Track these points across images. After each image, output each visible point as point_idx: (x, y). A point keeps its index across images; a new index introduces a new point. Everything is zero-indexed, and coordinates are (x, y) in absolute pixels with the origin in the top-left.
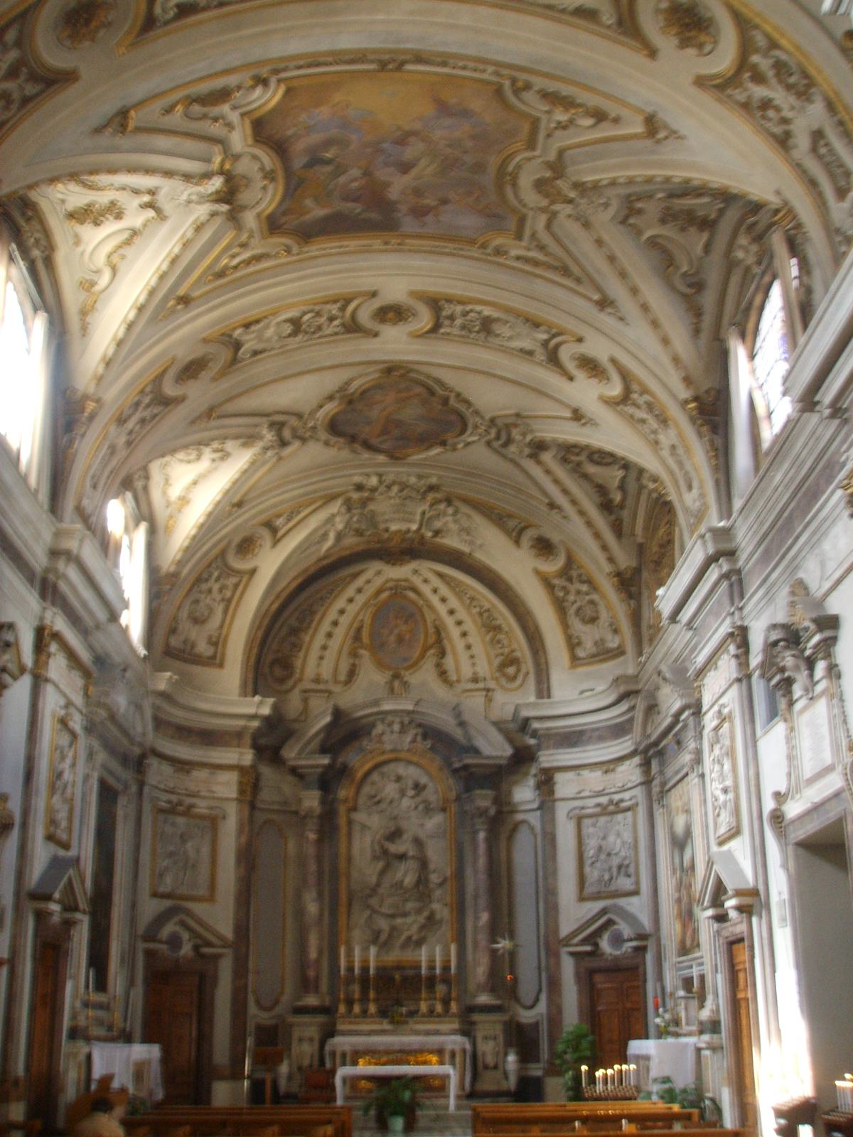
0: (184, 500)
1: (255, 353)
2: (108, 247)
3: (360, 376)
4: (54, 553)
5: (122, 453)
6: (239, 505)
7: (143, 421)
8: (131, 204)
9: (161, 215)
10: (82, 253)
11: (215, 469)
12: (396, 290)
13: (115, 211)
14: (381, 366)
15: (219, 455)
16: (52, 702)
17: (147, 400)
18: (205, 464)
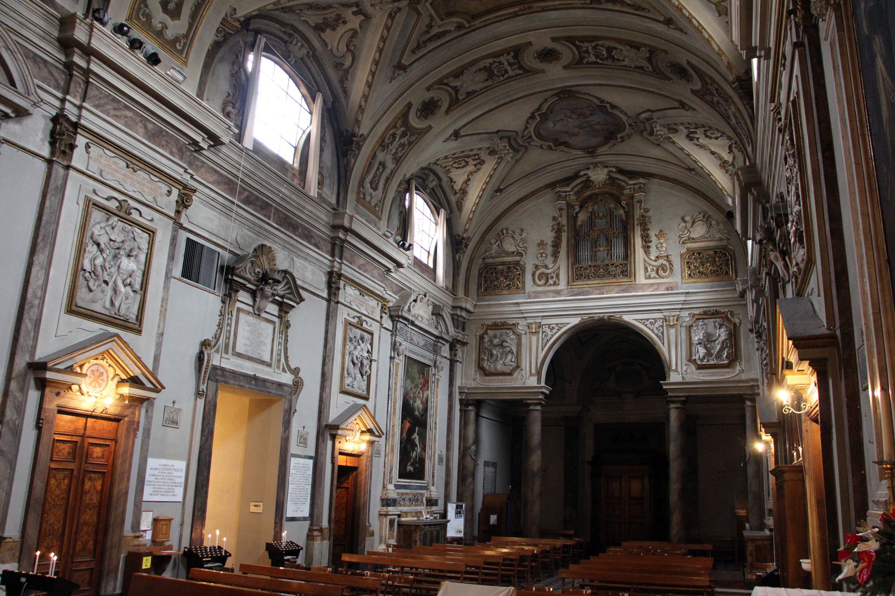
0: (464, 192)
1: (469, 94)
2: (345, 40)
3: (546, 100)
4: (335, 228)
5: (390, 165)
6: (499, 190)
7: (402, 145)
8: (348, 14)
9: (368, 17)
10: (331, 50)
11: (479, 169)
12: (542, 40)
13: (339, 20)
14: (554, 92)
15: (478, 161)
16: (343, 314)
17: (399, 132)
18: (470, 168)
